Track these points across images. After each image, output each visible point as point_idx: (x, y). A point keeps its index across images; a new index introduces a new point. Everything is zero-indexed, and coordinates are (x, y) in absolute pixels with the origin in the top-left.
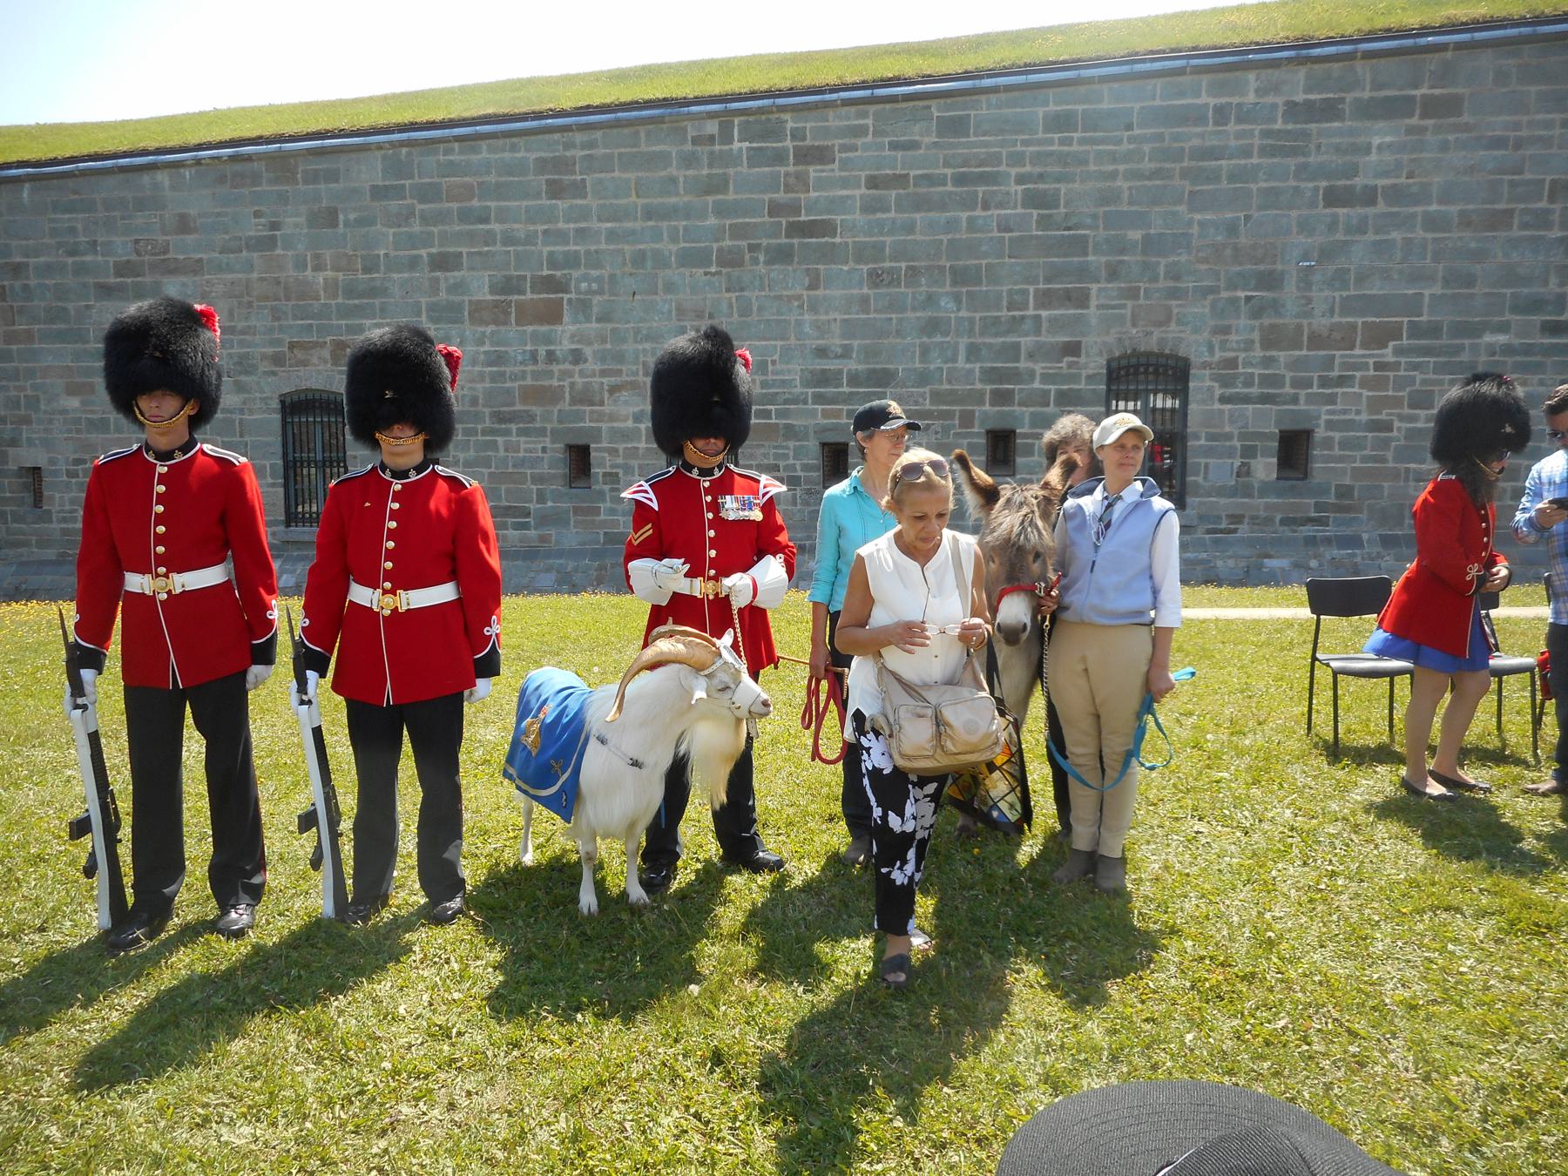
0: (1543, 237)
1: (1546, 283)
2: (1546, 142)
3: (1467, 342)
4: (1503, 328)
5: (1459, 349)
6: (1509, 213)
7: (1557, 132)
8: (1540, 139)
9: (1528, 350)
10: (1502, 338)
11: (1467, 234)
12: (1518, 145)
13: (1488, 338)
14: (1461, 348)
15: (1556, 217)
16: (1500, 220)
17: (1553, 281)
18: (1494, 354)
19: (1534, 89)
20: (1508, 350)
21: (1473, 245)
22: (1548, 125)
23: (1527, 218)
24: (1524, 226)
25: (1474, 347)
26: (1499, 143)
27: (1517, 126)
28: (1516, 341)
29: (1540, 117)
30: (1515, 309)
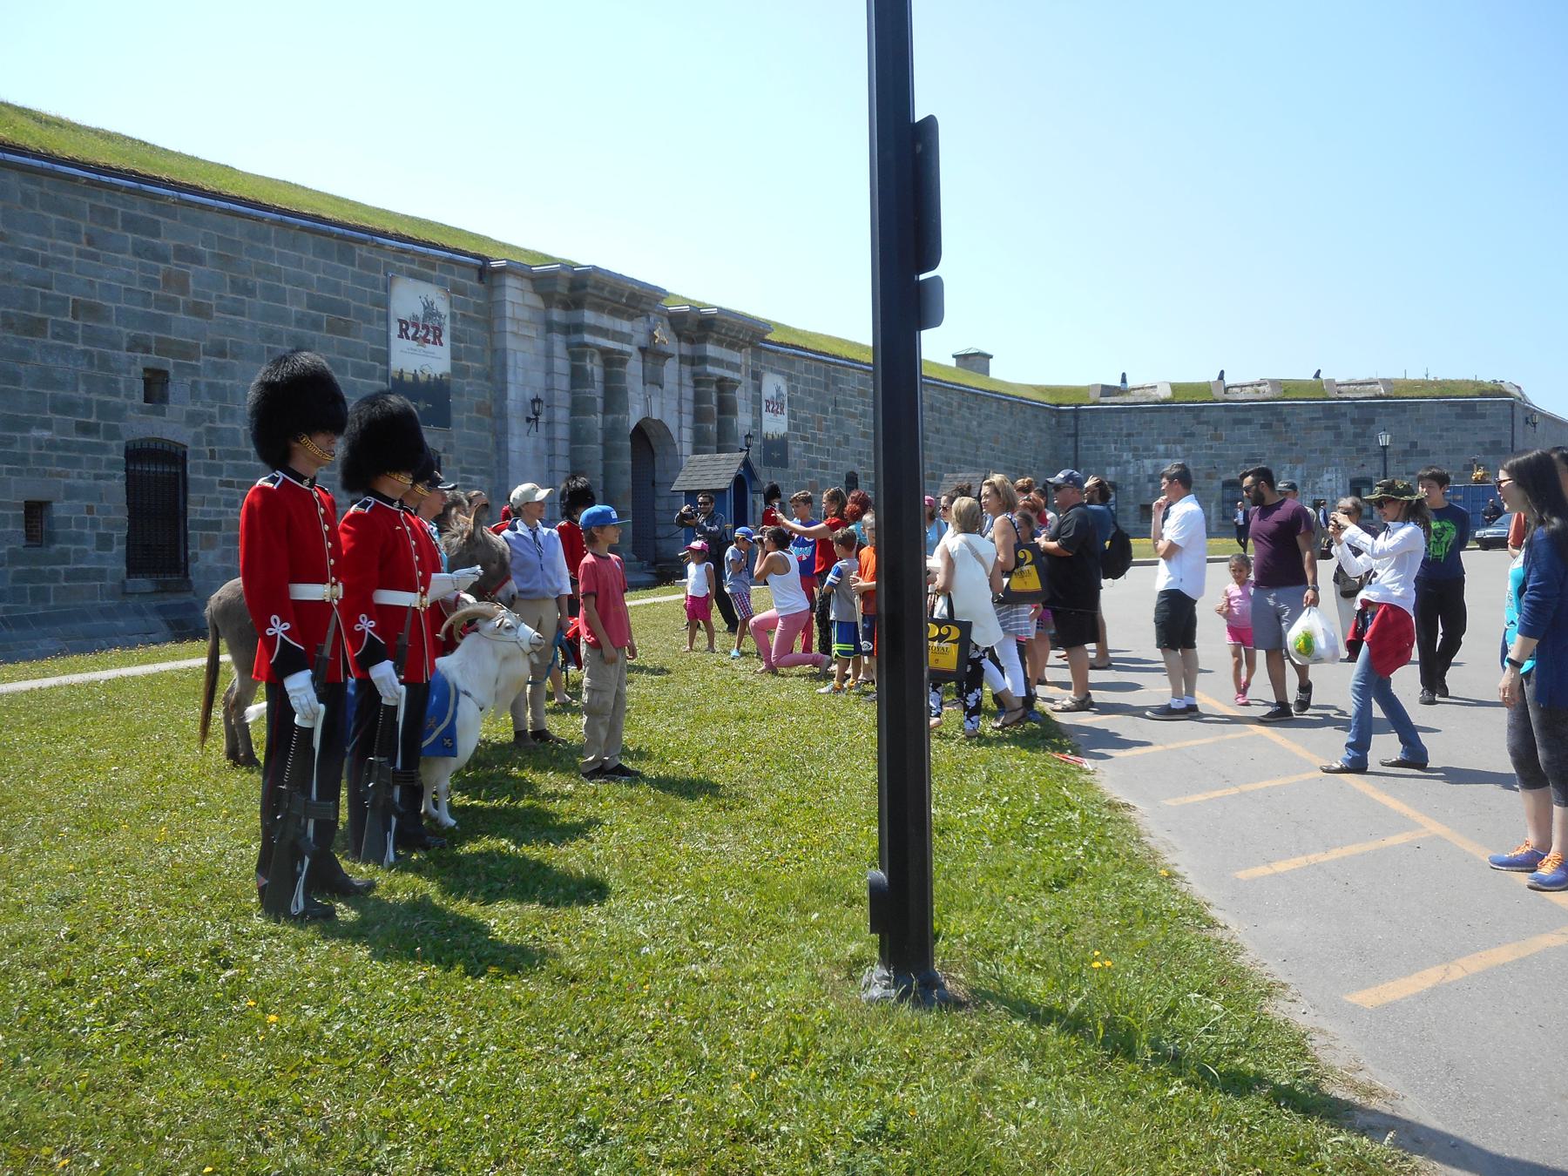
0: (70, 348)
1: (76, 390)
2: (66, 265)
3: (18, 435)
4: (46, 425)
5: (12, 441)
6: (43, 322)
7: (74, 258)
8: (61, 262)
9: (67, 446)
10: (47, 434)
11: (10, 335)
12: (46, 262)
13: (35, 433)
14: (12, 441)
15: (79, 332)
16: (35, 327)
17: (82, 388)
18: (40, 448)
19: (54, 217)
20: (52, 445)
21: (16, 346)
22: (67, 251)
23: (58, 330)
24: (56, 336)
25: (25, 441)
26: (30, 258)
27: (43, 246)
28: (58, 438)
29: (60, 242)
30: (54, 409)
